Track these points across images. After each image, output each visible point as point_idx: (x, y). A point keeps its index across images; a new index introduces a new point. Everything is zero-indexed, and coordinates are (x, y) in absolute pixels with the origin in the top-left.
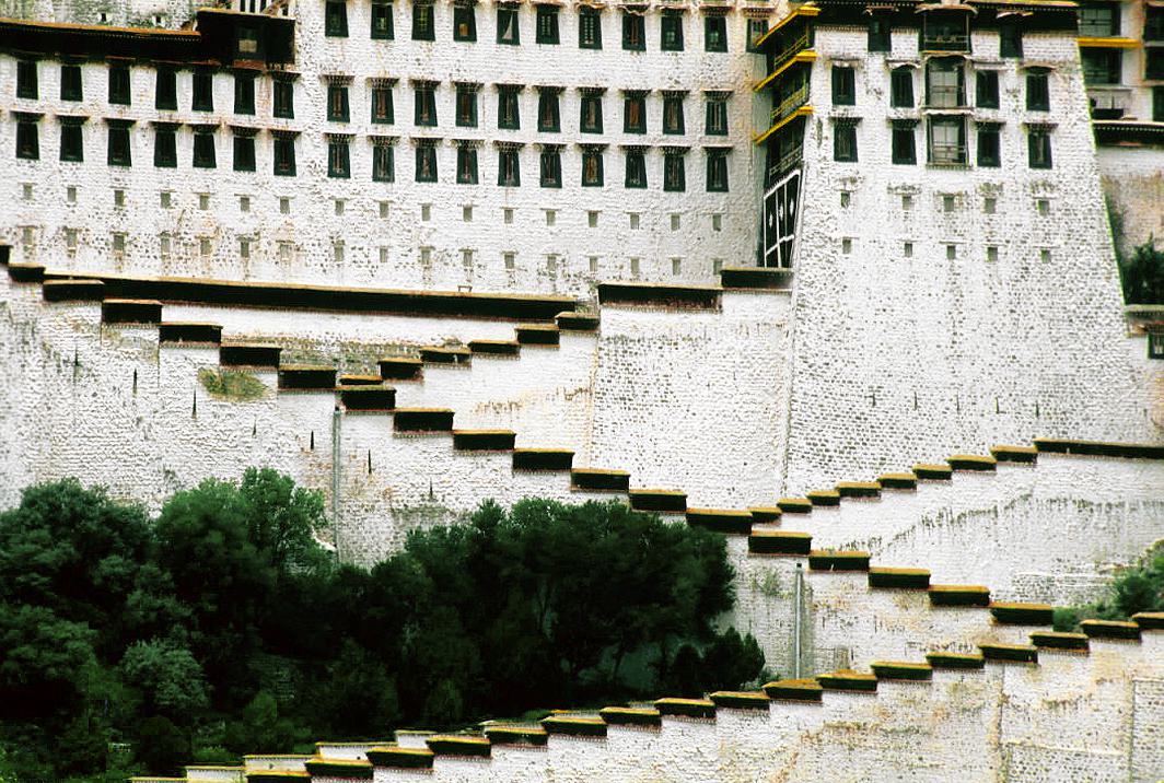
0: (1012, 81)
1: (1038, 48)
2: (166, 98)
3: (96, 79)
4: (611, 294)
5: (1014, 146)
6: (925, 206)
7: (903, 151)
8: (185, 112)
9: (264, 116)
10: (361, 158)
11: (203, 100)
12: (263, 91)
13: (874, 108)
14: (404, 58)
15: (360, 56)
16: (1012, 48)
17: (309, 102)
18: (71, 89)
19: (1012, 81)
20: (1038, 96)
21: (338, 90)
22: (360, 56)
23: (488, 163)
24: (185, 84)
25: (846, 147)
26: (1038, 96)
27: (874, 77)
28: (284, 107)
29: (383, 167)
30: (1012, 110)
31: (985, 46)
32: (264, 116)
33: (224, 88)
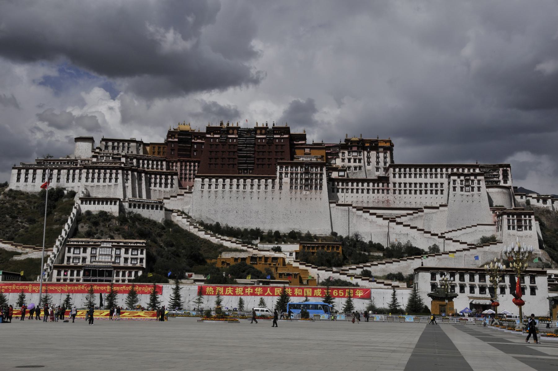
0: (476, 181)
1: (479, 178)
2: (374, 186)
4: (426, 207)
5: (476, 189)
6: (464, 197)
7: (462, 190)
8: (376, 187)
9: (385, 187)
12: (385, 185)
13: (458, 185)
14: (403, 180)
16: (475, 178)
17: (391, 186)
19: (476, 181)
20: (479, 183)
21: (394, 184)
22: (397, 180)
24: (376, 185)
26: (479, 183)
27: (458, 181)
28: (388, 186)
30: (476, 185)
31: (472, 178)
32: (385, 187)
33: (381, 185)
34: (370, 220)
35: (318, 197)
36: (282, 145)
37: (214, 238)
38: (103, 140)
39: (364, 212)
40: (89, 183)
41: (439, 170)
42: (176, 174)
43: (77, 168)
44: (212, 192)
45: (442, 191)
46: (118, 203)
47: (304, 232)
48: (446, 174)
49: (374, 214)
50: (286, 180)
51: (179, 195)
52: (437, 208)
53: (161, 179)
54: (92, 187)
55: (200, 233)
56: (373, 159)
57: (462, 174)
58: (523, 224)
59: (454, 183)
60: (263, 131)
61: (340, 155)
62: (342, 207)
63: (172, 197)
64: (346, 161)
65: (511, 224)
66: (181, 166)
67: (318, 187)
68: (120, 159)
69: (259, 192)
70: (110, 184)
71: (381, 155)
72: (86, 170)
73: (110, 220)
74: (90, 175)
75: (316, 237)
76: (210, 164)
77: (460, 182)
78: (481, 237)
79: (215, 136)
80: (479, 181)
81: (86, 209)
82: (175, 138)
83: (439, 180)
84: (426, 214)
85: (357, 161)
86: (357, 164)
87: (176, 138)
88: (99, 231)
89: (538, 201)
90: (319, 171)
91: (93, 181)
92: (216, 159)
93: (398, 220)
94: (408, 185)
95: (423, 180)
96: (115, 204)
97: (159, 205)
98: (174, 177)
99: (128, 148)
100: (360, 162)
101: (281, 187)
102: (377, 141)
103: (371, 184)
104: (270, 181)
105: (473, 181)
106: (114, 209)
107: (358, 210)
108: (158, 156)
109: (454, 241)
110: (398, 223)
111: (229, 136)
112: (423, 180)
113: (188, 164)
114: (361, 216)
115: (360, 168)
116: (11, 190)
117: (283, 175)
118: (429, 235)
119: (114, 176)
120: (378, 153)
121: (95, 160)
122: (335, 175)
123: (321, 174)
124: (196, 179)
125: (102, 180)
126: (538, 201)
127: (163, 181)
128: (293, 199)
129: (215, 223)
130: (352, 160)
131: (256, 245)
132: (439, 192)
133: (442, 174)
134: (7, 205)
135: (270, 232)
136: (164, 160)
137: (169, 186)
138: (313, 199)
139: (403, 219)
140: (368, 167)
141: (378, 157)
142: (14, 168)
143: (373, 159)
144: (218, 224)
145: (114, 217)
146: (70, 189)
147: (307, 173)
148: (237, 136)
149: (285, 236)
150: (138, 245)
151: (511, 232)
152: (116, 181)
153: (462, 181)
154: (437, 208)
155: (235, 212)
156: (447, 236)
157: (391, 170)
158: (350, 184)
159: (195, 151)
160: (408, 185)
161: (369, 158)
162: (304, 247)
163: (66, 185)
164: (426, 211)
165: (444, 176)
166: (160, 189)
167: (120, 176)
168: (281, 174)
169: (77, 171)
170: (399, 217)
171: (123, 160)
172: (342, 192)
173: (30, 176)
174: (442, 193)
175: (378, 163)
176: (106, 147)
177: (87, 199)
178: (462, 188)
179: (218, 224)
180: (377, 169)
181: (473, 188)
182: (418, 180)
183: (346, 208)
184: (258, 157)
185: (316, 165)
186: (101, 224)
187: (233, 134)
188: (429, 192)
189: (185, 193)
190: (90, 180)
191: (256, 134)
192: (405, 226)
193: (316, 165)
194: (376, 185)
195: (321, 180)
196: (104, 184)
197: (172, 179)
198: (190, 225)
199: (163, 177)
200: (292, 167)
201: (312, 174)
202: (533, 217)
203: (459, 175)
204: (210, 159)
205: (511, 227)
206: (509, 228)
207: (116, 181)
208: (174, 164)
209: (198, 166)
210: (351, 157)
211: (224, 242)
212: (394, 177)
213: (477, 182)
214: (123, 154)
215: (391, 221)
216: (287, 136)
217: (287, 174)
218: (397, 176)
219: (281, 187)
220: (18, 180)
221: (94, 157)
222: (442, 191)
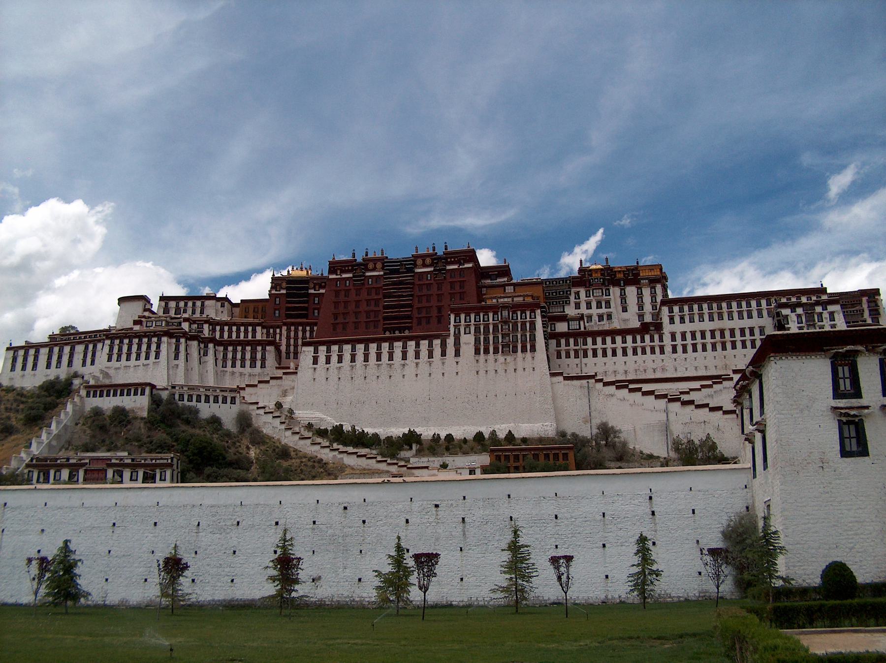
0: (826, 315)
1: (831, 308)
2: (634, 341)
3: (619, 339)
8: (639, 343)
10: (680, 349)
11: (643, 341)
12: (656, 337)
14: (688, 327)
15: (678, 328)
16: (825, 309)
18: (614, 342)
19: (826, 315)
22: (678, 328)
23: (709, 347)
24: (638, 338)
28: (661, 340)
29: (685, 351)
31: (819, 309)
33: (647, 338)
34: (632, 402)
38: (162, 298)
39: (618, 388)
40: (114, 363)
46: (148, 390)
49: (639, 389)
50: (468, 340)
55: (302, 442)
57: (799, 305)
60: (428, 261)
61: (572, 298)
62: (575, 382)
64: (583, 305)
68: (180, 324)
69: (417, 364)
73: (129, 422)
75: (524, 440)
77: (795, 318)
79: (344, 276)
80: (832, 314)
81: (94, 405)
82: (282, 288)
86: (603, 310)
87: (283, 289)
90: (528, 319)
93: (685, 398)
96: (143, 394)
98: (268, 348)
99: (202, 312)
100: (608, 303)
101: (457, 353)
102: (636, 268)
103: (629, 338)
104: (437, 342)
106: (139, 404)
107: (606, 384)
108: (256, 321)
111: (368, 274)
115: (609, 317)
119: (154, 347)
120: (639, 289)
121: (137, 328)
122: (562, 327)
123: (533, 324)
124: (305, 349)
127: (248, 356)
128: (482, 373)
130: (594, 304)
131: (408, 461)
135: (436, 438)
136: (259, 325)
137: (259, 363)
139: (693, 396)
140: (625, 315)
141: (640, 296)
145: (136, 418)
148: (382, 273)
149: (465, 441)
150: (162, 461)
153: (799, 316)
157: (665, 310)
161: (623, 298)
162: (498, 458)
165: (765, 313)
167: (164, 347)
170: (688, 393)
171: (185, 326)
172: (576, 356)
173: (31, 360)
175: (641, 307)
176: (166, 310)
183: (584, 382)
184: (420, 305)
185: (523, 307)
187: (374, 269)
189: (284, 374)
191: (415, 266)
193: (523, 307)
196: (138, 363)
199: (248, 348)
203: (793, 307)
211: (344, 456)
212: (672, 320)
213: (828, 316)
214: (186, 316)
215: (670, 400)
216: (470, 265)
219: (457, 353)
220: (13, 368)
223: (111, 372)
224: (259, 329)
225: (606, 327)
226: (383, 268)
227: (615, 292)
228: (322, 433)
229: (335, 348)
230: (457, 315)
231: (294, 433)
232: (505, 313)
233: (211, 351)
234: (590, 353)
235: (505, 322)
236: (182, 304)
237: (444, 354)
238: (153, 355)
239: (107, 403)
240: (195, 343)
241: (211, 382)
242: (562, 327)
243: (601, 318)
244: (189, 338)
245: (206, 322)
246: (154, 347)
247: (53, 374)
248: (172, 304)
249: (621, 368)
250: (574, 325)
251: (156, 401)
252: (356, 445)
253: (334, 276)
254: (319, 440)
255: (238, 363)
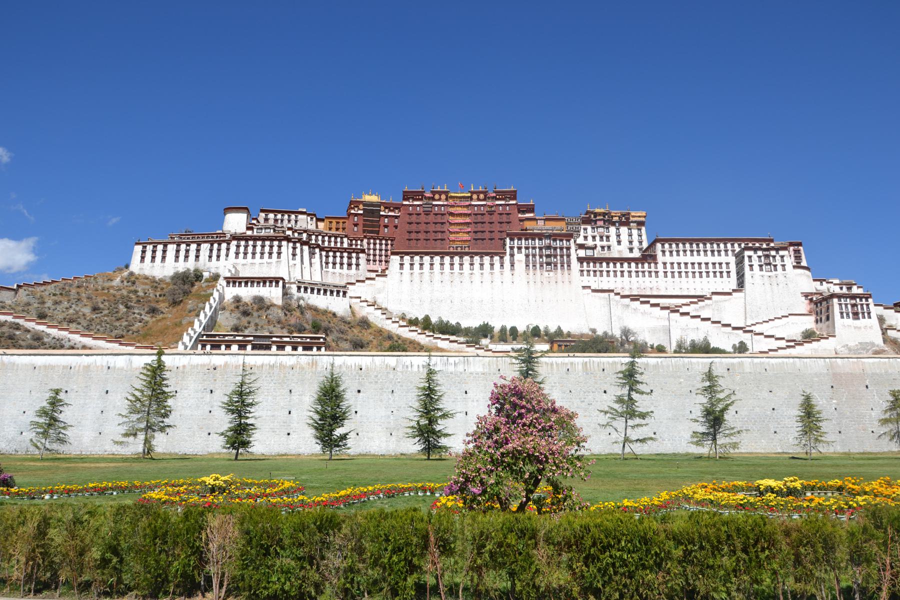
1: (781, 253)
2: (637, 267)
5: (779, 268)
6: (766, 278)
7: (761, 270)
8: (640, 269)
9: (653, 269)
12: (653, 265)
13: (756, 262)
14: (675, 259)
15: (668, 258)
16: (777, 253)
17: (660, 267)
19: (778, 258)
21: (665, 264)
24: (640, 265)
25: (752, 270)
27: (755, 257)
31: (773, 253)
32: (653, 269)
33: (646, 265)
34: (642, 311)
35: (567, 280)
36: (508, 214)
37: (424, 336)
39: (632, 300)
41: (722, 246)
42: (363, 251)
43: (224, 241)
44: (415, 275)
45: (728, 272)
47: (553, 329)
48: (733, 251)
49: (648, 302)
50: (520, 257)
51: (367, 279)
52: (729, 294)
53: (342, 257)
54: (243, 265)
56: (624, 237)
57: (760, 249)
58: (860, 310)
59: (750, 261)
60: (482, 196)
63: (358, 281)
64: (590, 238)
65: (844, 310)
66: (369, 244)
67: (566, 265)
68: (284, 232)
70: (270, 261)
71: (635, 232)
72: (234, 243)
73: (268, 308)
74: (242, 249)
75: (569, 335)
76: (410, 240)
78: (803, 329)
83: (723, 259)
84: (716, 302)
85: (605, 238)
86: (605, 243)
88: (252, 324)
89: (841, 288)
91: (245, 257)
92: (417, 232)
93: (681, 310)
94: (683, 266)
95: (702, 259)
97: (340, 291)
98: (361, 255)
99: (296, 222)
100: (608, 237)
104: (496, 258)
105: (774, 257)
106: (273, 294)
107: (623, 297)
109: (766, 337)
110: (683, 314)
111: (434, 203)
112: (702, 259)
113: (378, 241)
114: (628, 306)
115: (609, 247)
116: (132, 274)
117: (516, 250)
118: (730, 329)
119: (275, 249)
121: (249, 233)
122: (582, 253)
123: (568, 249)
124: (392, 257)
125: (258, 255)
126: (841, 288)
127: (345, 260)
128: (531, 283)
129: (423, 316)
130: (598, 238)
131: (487, 346)
132: (725, 274)
133: (726, 251)
134: (125, 292)
136: (346, 236)
137: (354, 267)
138: (560, 283)
139: (684, 309)
141: (630, 235)
142: (137, 244)
143: (624, 237)
144: (427, 319)
145: (273, 305)
146: (213, 271)
147: (549, 247)
151: (845, 320)
152: (279, 257)
153: (759, 257)
154: (729, 294)
155: (449, 301)
156: (757, 329)
158: (604, 264)
159: (386, 226)
160: (683, 266)
163: (208, 264)
164: (714, 297)
166: (341, 271)
167: (284, 249)
168: (512, 248)
169: (224, 245)
171: (289, 233)
173: (159, 254)
174: (729, 276)
175: (631, 242)
176: (266, 220)
177: (233, 281)
178: (761, 266)
179: (427, 319)
180: (631, 250)
181: (775, 266)
182: (696, 259)
183: (606, 294)
186: (255, 314)
187: (440, 200)
188: (711, 274)
190: (241, 255)
191: (471, 198)
192: (693, 317)
194: (640, 265)
195: (569, 256)
196: (261, 261)
197: (358, 258)
198: (387, 319)
199: (345, 254)
200: (526, 239)
201: (555, 249)
202: (870, 300)
203: (756, 250)
204: (410, 232)
205: (845, 315)
206: (842, 317)
207: (279, 257)
208: (359, 242)
209: (392, 245)
210: (596, 234)
212: (664, 252)
214: (290, 226)
216: (514, 202)
217: (519, 248)
218: (667, 253)
219: (512, 265)
221: (248, 228)
222: (728, 272)
223: (239, 268)
224: (345, 240)
225: (607, 256)
226: (447, 199)
227: (613, 230)
228: (413, 322)
229: (417, 258)
230: (512, 240)
231: (393, 322)
232: (548, 241)
233: (317, 256)
234: (605, 273)
235: (549, 247)
236: (279, 216)
237: (502, 266)
238: (275, 255)
239: (247, 293)
240: (306, 248)
241: (317, 278)
242: (582, 253)
243: (603, 247)
244: (303, 243)
245: (305, 231)
246: (275, 249)
247: (181, 266)
248: (271, 216)
249: (635, 286)
250: (590, 253)
251: (285, 294)
252: (443, 333)
253: (407, 203)
254: (413, 328)
255: (338, 266)
